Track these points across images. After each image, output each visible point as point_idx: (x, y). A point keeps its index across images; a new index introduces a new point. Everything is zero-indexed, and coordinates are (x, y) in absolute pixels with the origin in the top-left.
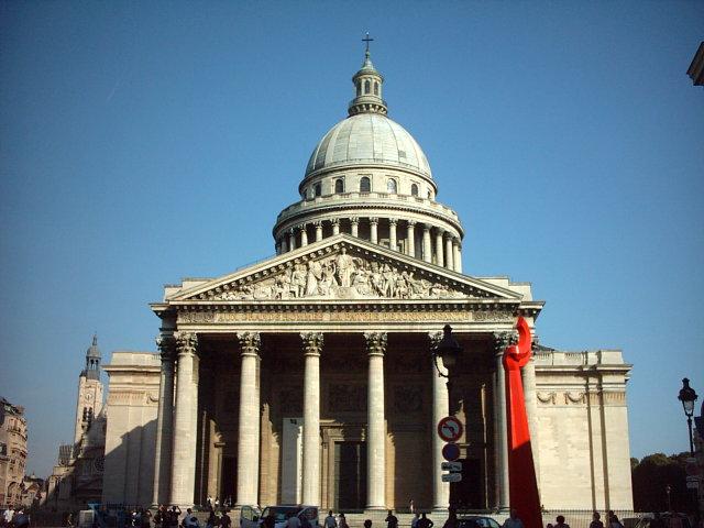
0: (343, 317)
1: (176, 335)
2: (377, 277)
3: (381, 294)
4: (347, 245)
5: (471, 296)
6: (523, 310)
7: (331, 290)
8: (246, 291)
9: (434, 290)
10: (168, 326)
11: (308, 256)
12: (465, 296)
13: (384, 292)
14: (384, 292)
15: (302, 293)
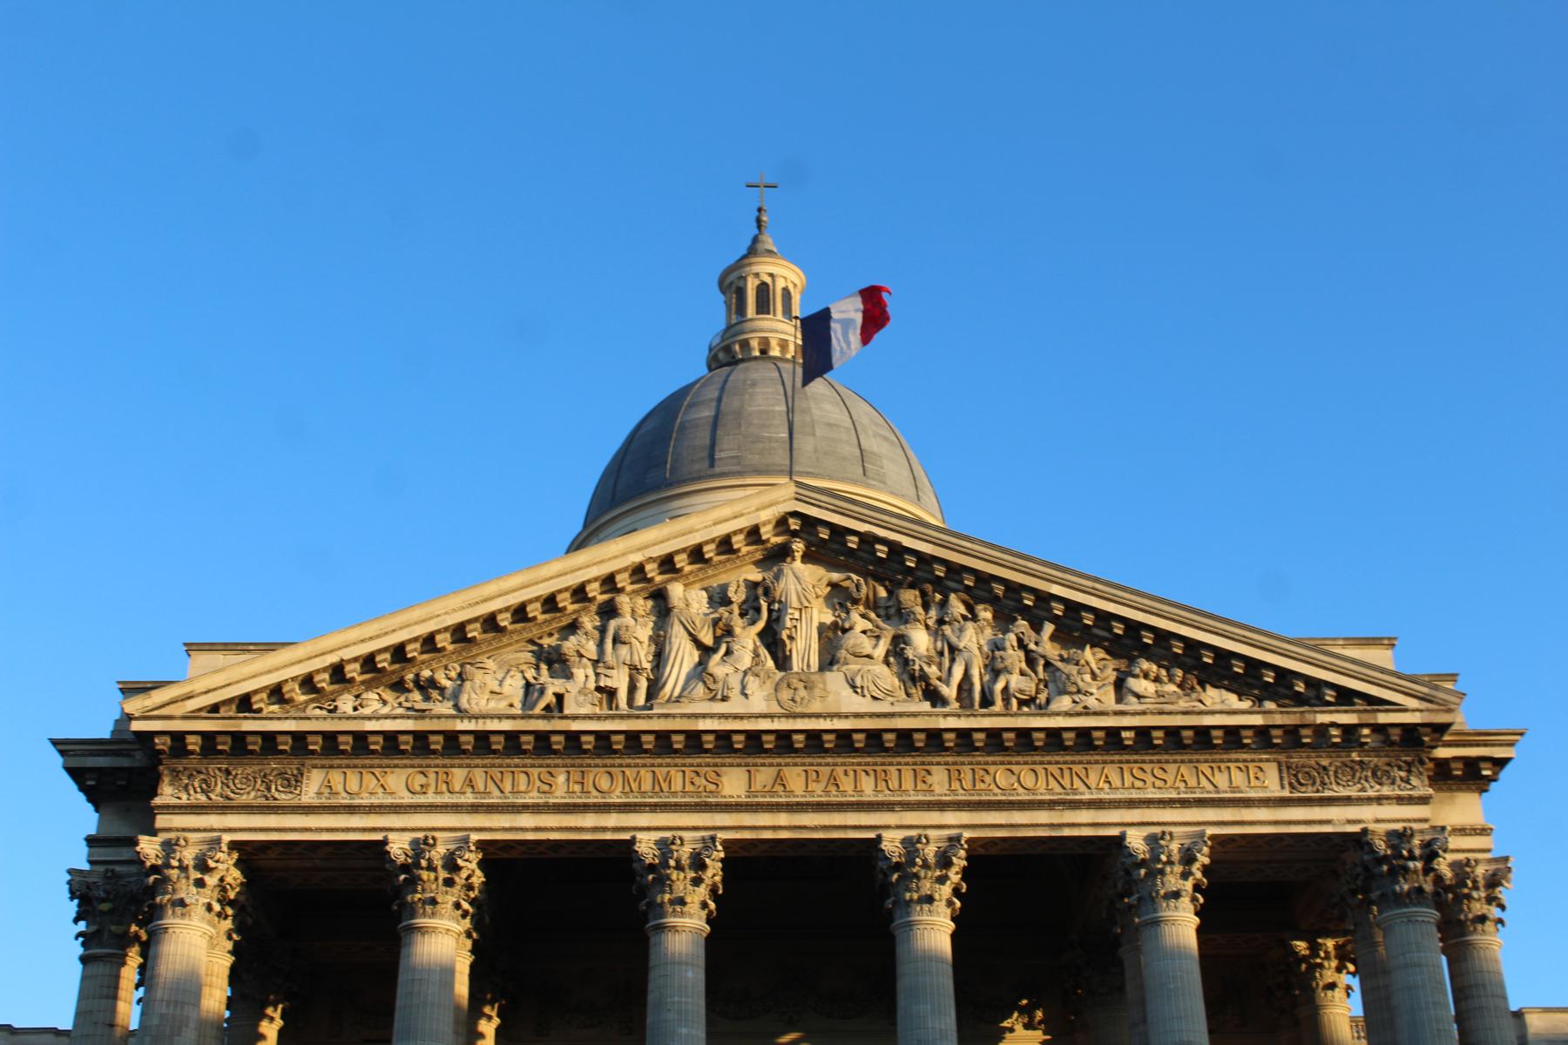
0: (797, 780)
1: (149, 847)
2: (921, 640)
3: (933, 696)
4: (809, 523)
5: (1270, 705)
6: (1443, 766)
7: (753, 684)
8: (427, 687)
9: (1133, 683)
10: (119, 829)
11: (667, 564)
12: (1246, 704)
13: (950, 692)
14: (950, 692)
15: (641, 698)
